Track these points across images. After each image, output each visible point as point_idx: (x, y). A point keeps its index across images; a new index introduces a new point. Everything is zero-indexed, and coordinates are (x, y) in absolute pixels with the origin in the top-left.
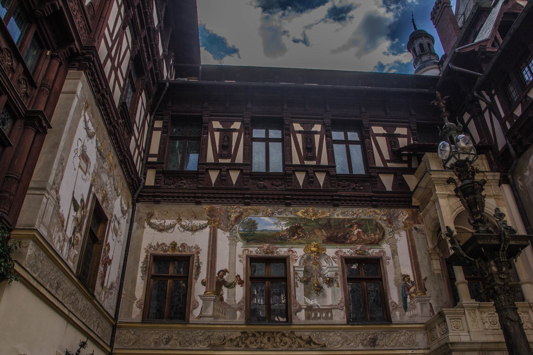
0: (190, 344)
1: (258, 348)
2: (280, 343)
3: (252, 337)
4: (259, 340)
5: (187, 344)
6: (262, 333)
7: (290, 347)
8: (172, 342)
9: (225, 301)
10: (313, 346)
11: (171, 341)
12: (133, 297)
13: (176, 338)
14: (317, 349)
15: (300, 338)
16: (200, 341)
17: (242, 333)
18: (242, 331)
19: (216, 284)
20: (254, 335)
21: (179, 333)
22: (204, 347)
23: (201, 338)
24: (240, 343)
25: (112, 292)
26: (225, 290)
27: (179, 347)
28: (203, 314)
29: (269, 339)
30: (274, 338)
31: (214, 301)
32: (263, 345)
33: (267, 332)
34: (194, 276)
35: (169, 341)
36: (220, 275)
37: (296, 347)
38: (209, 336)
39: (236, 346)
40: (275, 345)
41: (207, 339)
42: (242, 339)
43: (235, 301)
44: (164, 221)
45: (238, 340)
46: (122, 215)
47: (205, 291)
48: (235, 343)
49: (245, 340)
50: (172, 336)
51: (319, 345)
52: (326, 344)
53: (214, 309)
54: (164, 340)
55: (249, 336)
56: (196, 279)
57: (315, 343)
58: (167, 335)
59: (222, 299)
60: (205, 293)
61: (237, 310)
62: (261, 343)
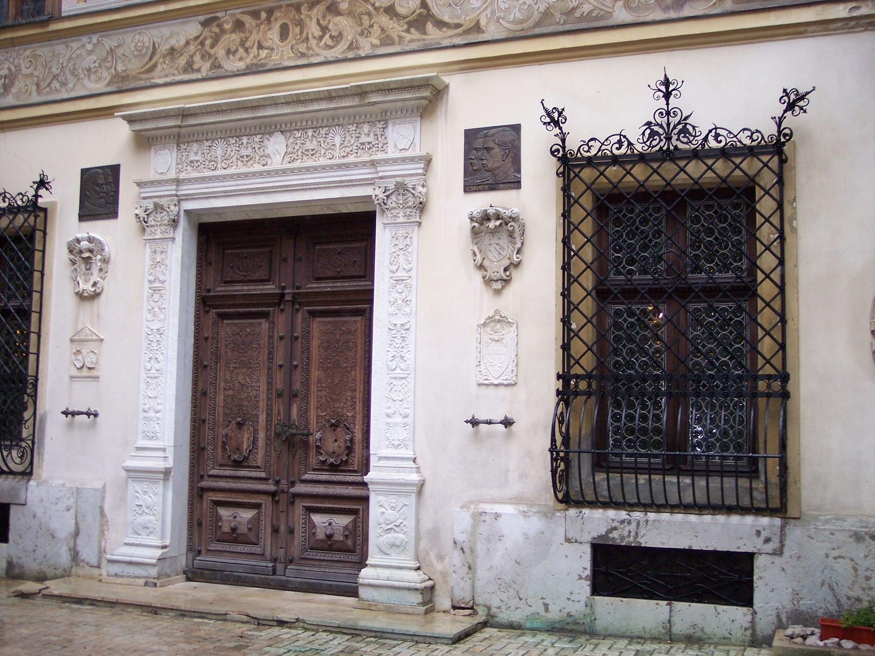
0: (64, 84)
1: (248, 68)
2: (321, 38)
3: (233, 31)
4: (254, 37)
5: (56, 84)
6: (264, 15)
7: (351, 47)
8: (19, 85)
10: (433, 33)
11: (17, 83)
13: (28, 72)
14: (446, 43)
15: (390, 10)
16: (89, 70)
17: (205, 24)
18: (202, 18)
20: (239, 25)
21: (36, 57)
22: (100, 87)
23: (89, 61)
24: (197, 58)
27: (35, 99)
29: (284, 33)
30: (301, 24)
32: (264, 53)
33: (281, 7)
35: (12, 84)
37: (373, 46)
38: (112, 51)
39: (185, 71)
40: (302, 48)
41: (105, 60)
42: (202, 44)
45: (192, 48)
48: (182, 61)
49: (213, 46)
50: (18, 67)
51: (458, 26)
52: (483, 22)
55: (223, 31)
57: (440, 24)
58: (6, 66)
62: (260, 47)
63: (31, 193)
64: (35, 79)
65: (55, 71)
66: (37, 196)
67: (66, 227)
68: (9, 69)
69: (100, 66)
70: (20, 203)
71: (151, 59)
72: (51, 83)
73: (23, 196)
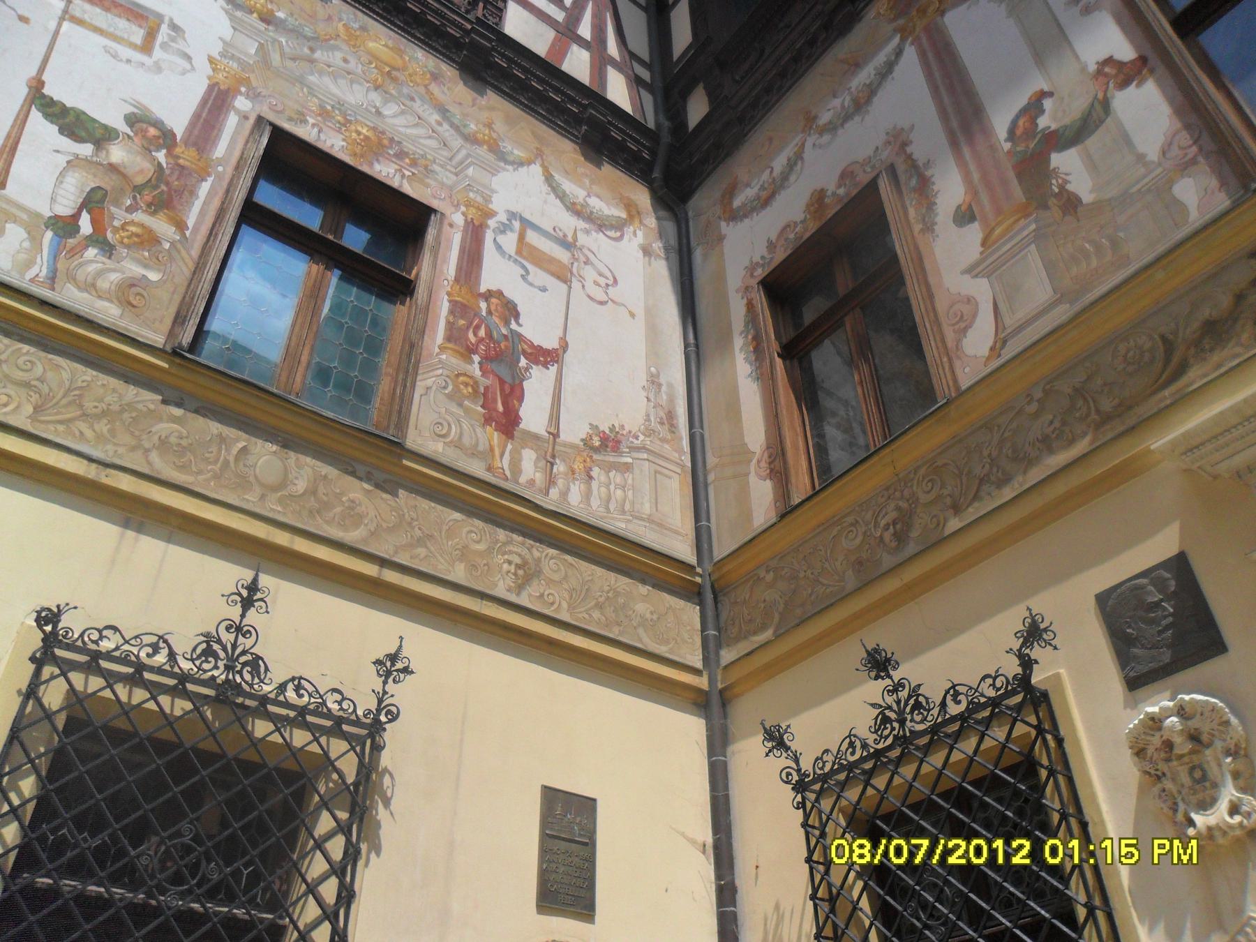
9: (1087, 197)
12: (741, 453)
19: (1019, 176)
25: (627, 468)
26: (1066, 162)
28: (1010, 321)
31: (1039, 237)
34: (917, 228)
36: (1019, 132)
38: (1079, 392)
43: (1141, 158)
44: (768, 171)
46: (582, 224)
47: (981, 236)
53: (1050, 267)
54: (887, 536)
56: (929, 228)
59: (1071, 203)
60: (983, 244)
61: (1171, 183)
63: (1012, 667)
64: (948, 501)
65: (978, 471)
66: (1027, 664)
67: (1102, 724)
68: (898, 508)
69: (1064, 423)
70: (991, 693)
71: (1167, 361)
72: (977, 491)
73: (995, 679)
